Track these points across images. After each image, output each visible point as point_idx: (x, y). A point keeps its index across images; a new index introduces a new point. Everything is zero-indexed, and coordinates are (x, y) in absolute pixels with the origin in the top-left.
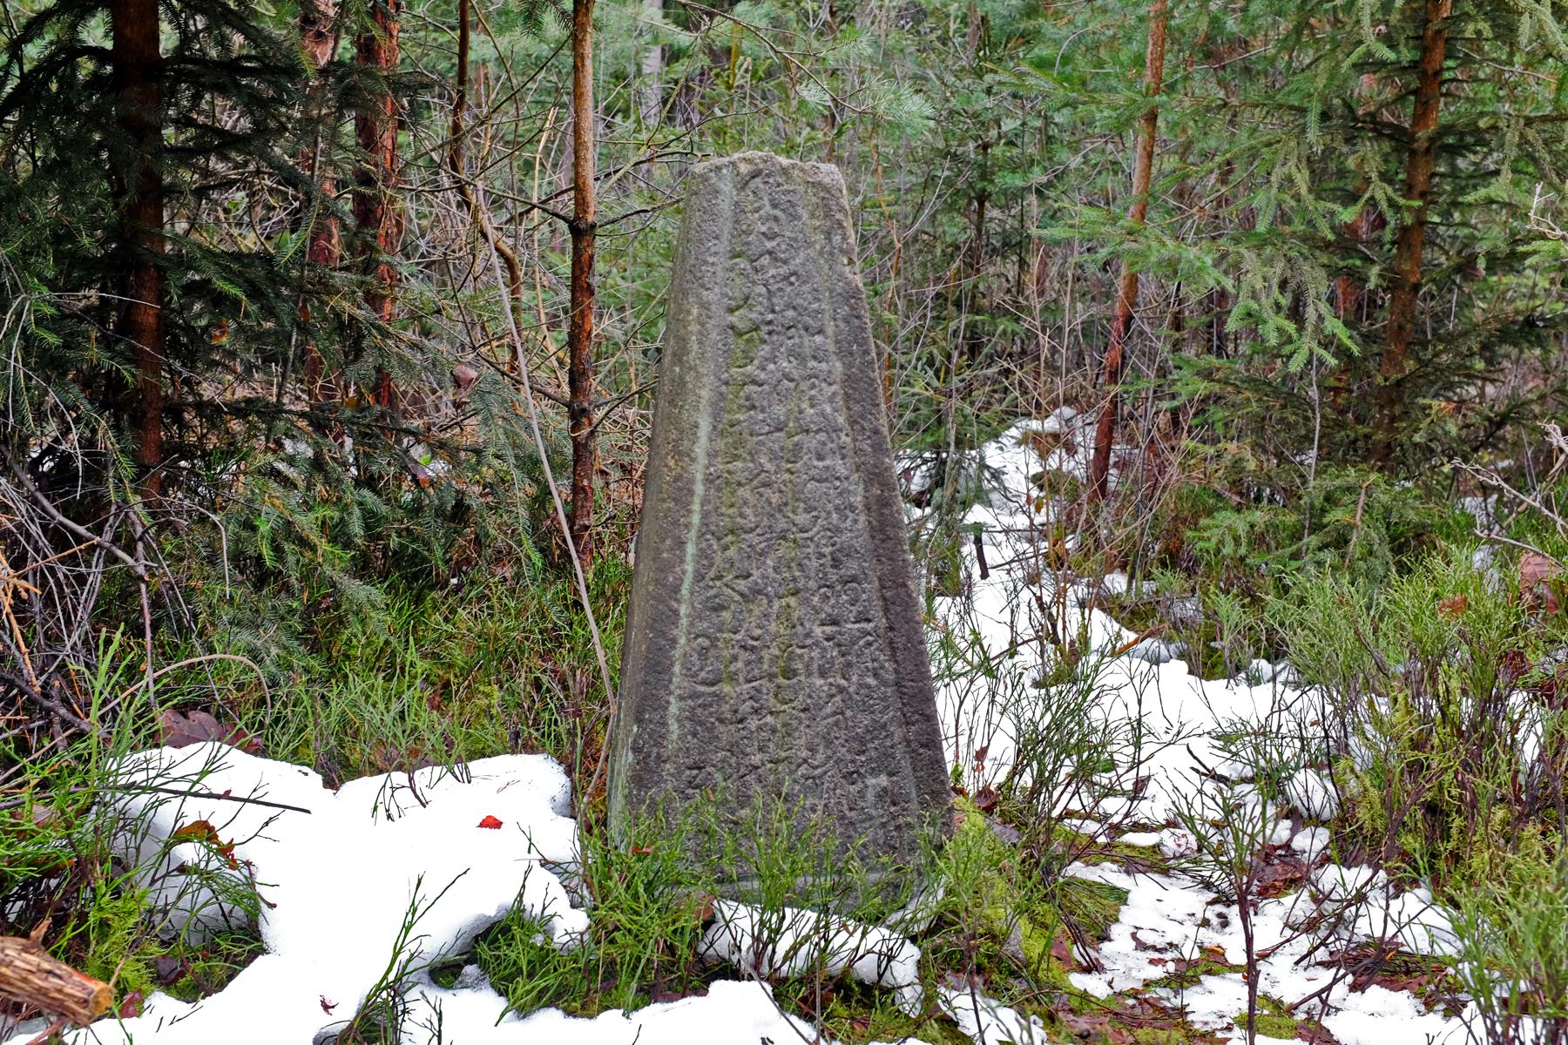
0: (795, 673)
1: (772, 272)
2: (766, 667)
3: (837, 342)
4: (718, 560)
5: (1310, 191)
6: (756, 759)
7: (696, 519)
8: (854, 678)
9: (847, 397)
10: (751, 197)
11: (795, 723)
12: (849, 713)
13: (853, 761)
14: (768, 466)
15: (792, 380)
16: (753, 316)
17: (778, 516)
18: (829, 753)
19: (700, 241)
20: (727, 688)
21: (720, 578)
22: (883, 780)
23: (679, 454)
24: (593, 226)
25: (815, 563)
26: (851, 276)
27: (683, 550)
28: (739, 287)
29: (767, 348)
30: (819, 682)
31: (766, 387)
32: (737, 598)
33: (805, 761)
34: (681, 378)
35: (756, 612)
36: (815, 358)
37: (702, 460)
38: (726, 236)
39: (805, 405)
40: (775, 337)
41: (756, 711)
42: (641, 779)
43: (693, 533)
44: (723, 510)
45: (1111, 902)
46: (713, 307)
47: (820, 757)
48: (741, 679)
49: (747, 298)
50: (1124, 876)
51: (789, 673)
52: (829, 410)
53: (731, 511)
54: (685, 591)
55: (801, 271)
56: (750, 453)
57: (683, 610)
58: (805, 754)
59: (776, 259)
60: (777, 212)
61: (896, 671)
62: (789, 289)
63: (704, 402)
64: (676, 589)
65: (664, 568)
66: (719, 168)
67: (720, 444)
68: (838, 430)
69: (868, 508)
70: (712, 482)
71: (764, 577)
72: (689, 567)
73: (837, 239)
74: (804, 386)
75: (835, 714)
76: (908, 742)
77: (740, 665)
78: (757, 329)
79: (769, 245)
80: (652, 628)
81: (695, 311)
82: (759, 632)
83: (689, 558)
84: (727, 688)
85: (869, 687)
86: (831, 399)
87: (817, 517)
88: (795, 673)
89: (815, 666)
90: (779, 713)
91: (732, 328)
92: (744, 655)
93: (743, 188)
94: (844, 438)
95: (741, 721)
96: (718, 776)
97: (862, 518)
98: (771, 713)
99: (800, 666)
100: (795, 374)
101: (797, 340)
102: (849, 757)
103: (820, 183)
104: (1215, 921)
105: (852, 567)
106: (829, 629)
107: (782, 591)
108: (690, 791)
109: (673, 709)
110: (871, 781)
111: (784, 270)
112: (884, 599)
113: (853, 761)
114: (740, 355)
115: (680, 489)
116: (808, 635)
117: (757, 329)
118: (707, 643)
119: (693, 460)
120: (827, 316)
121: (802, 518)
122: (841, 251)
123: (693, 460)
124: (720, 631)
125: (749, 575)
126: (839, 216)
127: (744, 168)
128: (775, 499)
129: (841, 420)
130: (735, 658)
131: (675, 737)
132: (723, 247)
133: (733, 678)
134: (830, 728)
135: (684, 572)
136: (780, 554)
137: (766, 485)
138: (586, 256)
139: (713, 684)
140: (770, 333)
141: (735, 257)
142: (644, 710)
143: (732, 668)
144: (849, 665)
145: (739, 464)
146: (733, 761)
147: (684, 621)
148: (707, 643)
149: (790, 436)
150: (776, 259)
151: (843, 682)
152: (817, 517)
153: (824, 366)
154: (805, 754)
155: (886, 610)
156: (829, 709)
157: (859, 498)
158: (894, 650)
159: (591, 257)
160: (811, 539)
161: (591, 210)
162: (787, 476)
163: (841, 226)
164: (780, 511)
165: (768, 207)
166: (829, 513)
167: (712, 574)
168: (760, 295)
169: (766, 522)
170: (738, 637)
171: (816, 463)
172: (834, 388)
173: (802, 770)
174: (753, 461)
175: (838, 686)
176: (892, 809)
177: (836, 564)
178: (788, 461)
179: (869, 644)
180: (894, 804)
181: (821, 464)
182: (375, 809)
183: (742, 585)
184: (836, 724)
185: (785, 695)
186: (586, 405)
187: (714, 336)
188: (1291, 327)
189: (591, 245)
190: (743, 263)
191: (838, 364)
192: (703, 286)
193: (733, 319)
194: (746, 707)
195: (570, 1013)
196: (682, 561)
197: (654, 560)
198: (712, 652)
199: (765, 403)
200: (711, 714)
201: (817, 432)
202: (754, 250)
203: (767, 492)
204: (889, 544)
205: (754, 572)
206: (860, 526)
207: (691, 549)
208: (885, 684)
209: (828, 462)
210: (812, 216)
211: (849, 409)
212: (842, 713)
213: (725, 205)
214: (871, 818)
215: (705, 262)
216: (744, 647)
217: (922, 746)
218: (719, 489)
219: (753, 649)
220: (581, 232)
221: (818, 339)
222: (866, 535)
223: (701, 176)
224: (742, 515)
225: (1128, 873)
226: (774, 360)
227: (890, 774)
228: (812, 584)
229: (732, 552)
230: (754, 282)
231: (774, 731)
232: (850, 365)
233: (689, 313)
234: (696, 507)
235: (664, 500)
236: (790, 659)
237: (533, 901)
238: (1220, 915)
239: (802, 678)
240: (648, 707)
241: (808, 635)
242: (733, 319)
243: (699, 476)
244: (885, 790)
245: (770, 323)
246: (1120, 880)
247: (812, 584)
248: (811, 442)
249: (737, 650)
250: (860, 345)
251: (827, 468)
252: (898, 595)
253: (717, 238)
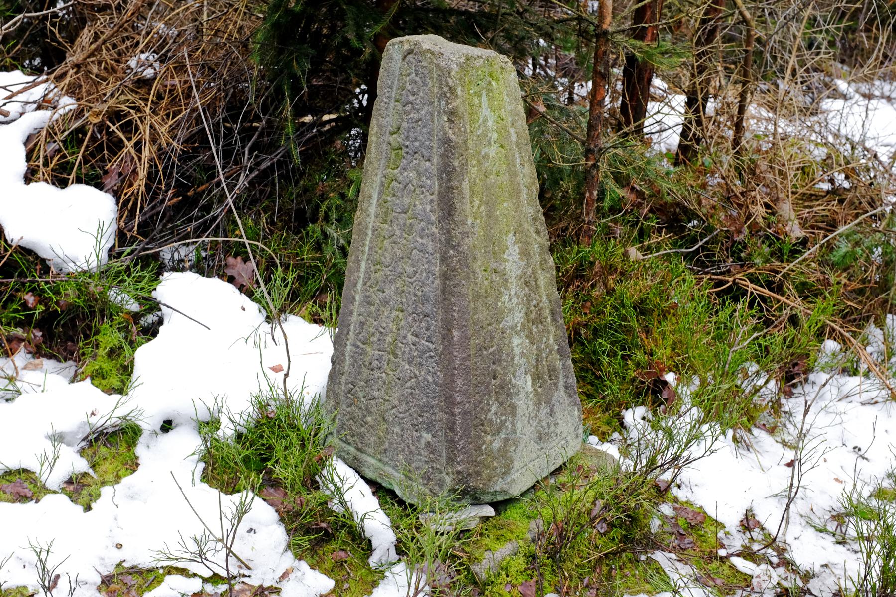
26: (447, 129)
41: (379, 368)
49: (399, 129)
57: (357, 298)
78: (401, 149)
79: (411, 98)
84: (369, 349)
102: (415, 416)
105: (428, 308)
106: (414, 339)
109: (349, 348)
110: (425, 435)
128: (399, 252)
136: (398, 285)
139: (364, 344)
151: (417, 372)
157: (437, 269)
179: (432, 357)
181: (420, 241)
184: (411, 393)
196: (359, 271)
207: (363, 265)
209: (424, 241)
221: (428, 164)
245: (407, 147)
250: (447, 175)
251: (423, 244)
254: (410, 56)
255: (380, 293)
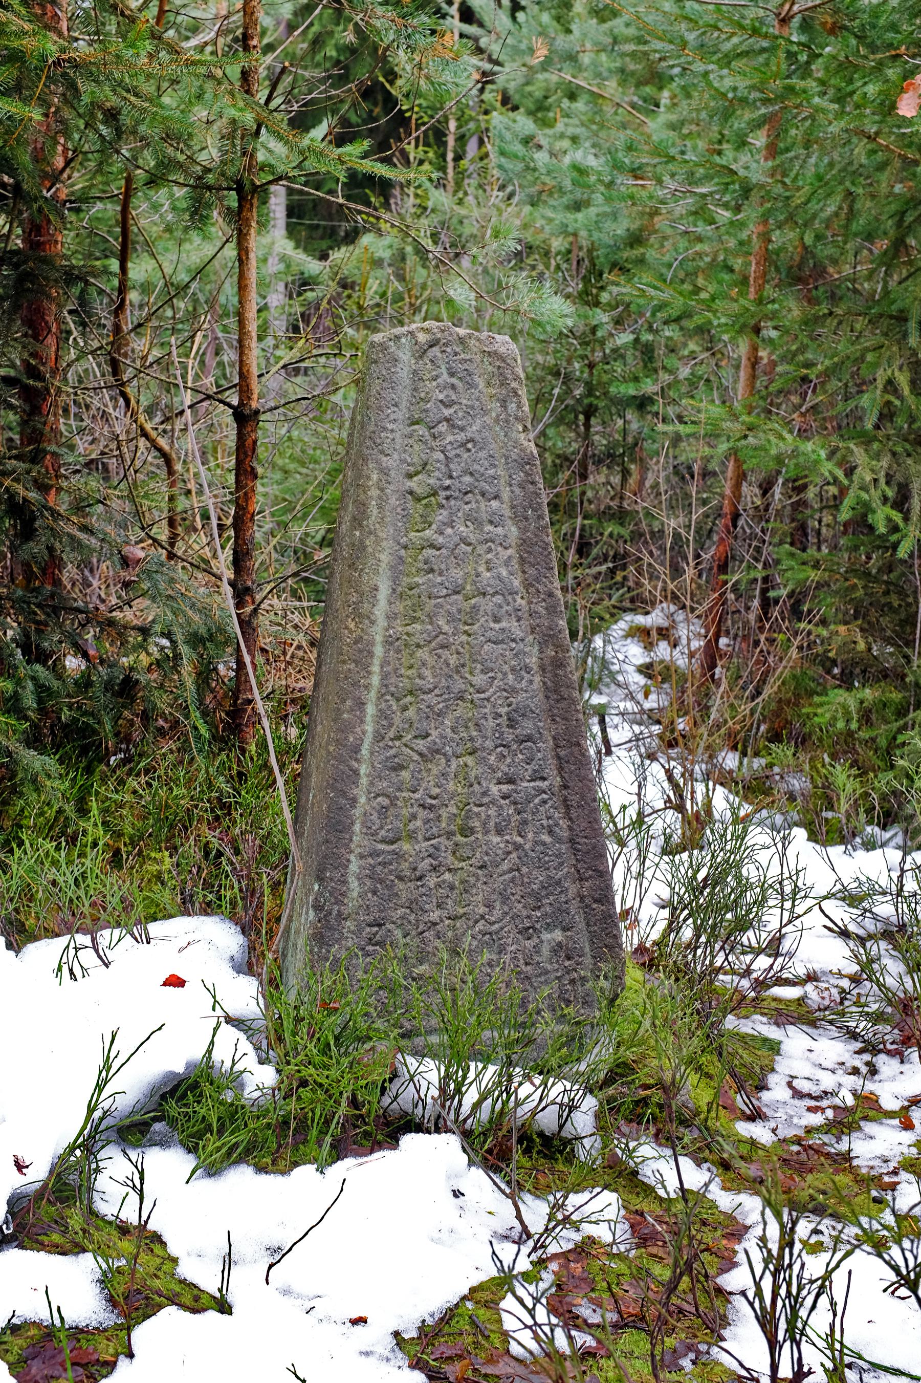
0: (472, 831)
1: (450, 438)
2: (444, 825)
3: (513, 507)
4: (397, 720)
5: (911, 392)
6: (435, 916)
7: (375, 680)
8: (530, 836)
9: (522, 560)
10: (429, 366)
11: (472, 880)
12: (525, 870)
13: (528, 917)
14: (446, 628)
15: (469, 544)
16: (431, 481)
17: (456, 677)
18: (506, 908)
19: (380, 408)
20: (406, 846)
21: (399, 738)
22: (558, 935)
23: (359, 616)
24: (257, 412)
25: (491, 723)
26: (526, 443)
27: (363, 711)
28: (417, 454)
29: (445, 513)
30: (496, 839)
31: (443, 551)
32: (416, 757)
33: (482, 917)
34: (362, 542)
35: (435, 771)
36: (491, 522)
37: (382, 622)
38: (404, 404)
39: (482, 568)
40: (453, 502)
41: (434, 869)
42: (322, 937)
43: (373, 694)
44: (403, 671)
45: (763, 1052)
46: (392, 473)
47: (497, 913)
48: (420, 838)
50: (774, 1028)
51: (466, 831)
52: (504, 573)
53: (410, 672)
54: (365, 751)
55: (477, 437)
56: (429, 616)
57: (363, 770)
58: (482, 910)
59: (453, 426)
60: (454, 380)
61: (570, 829)
62: (465, 455)
63: (383, 565)
64: (357, 749)
65: (345, 728)
66: (398, 338)
67: (400, 607)
68: (513, 593)
69: (543, 669)
70: (391, 644)
71: (442, 737)
72: (369, 728)
73: (512, 407)
74: (481, 549)
75: (511, 870)
76: (582, 898)
77: (419, 823)
78: (435, 494)
79: (447, 412)
80: (333, 788)
81: (375, 477)
82: (436, 791)
83: (368, 719)
84: (406, 846)
85: (544, 844)
86: (507, 563)
87: (494, 678)
88: (472, 831)
89: (492, 824)
90: (456, 870)
91: (411, 493)
92: (423, 814)
93: (421, 357)
94: (519, 600)
95: (420, 878)
96: (398, 933)
97: (537, 679)
98: (450, 870)
99: (477, 824)
100: (472, 538)
101: (474, 505)
102: (525, 913)
103: (495, 353)
104: (864, 1070)
105: (527, 727)
106: (505, 788)
107: (459, 750)
108: (370, 948)
109: (354, 867)
110: (546, 936)
111: (461, 437)
112: (559, 758)
113: (528, 917)
114: (419, 519)
115: (360, 651)
116: (485, 794)
117: (435, 494)
118: (385, 801)
119: (373, 622)
120: (502, 481)
121: (479, 679)
122: (517, 418)
123: (373, 622)
124: (400, 790)
125: (428, 735)
126: (514, 384)
127: (422, 338)
128: (453, 660)
129: (516, 583)
130: (414, 817)
131: (355, 894)
132: (401, 414)
133: (411, 836)
134: (506, 885)
135: (364, 733)
137: (443, 647)
138: (249, 442)
140: (447, 498)
141: (413, 424)
142: (325, 869)
143: (411, 826)
144: (525, 822)
145: (418, 626)
146: (412, 917)
147: (364, 781)
148: (385, 801)
149: (467, 599)
150: (453, 426)
151: (519, 840)
152: (494, 678)
153: (500, 530)
154: (482, 910)
155: (560, 769)
156: (505, 866)
157: (534, 660)
158: (568, 807)
159: (255, 442)
160: (488, 700)
161: (255, 396)
162: (464, 638)
163: (516, 394)
164: (458, 672)
165: (445, 376)
166: (505, 674)
167: (391, 734)
168: (438, 461)
169: (444, 683)
170: (417, 796)
171: (492, 625)
172: (510, 552)
173: (480, 926)
174: (431, 623)
175: (515, 843)
176: (567, 963)
177: (512, 723)
178: (466, 623)
179: (544, 802)
180: (569, 958)
181: (497, 626)
182: (60, 969)
183: (421, 745)
184: (513, 880)
185: (462, 852)
186: (249, 583)
187: (393, 501)
188: (897, 517)
189: (254, 430)
190: (421, 430)
191: (514, 529)
192: (382, 452)
193: (412, 484)
194: (425, 865)
195: (261, 1169)
196: (362, 722)
197: (335, 720)
198: (392, 811)
199: (443, 567)
200: (391, 872)
201: (493, 595)
202: (432, 417)
203: (445, 653)
204: (564, 704)
205: (432, 732)
206: (535, 686)
207: (370, 710)
208: (560, 841)
209: (504, 624)
210: (489, 384)
211: (524, 572)
212: (518, 870)
213: (403, 373)
214: (547, 972)
215: (384, 429)
216: (423, 806)
217: (596, 901)
218: (398, 651)
219: (431, 808)
220: (245, 418)
221: (495, 504)
222: (541, 696)
223: (381, 345)
224: (420, 676)
225: (777, 1024)
226: (451, 524)
227: (564, 929)
228: (489, 744)
229: (411, 713)
230: (432, 449)
231: (452, 888)
232: (525, 530)
233: (368, 478)
234: (376, 668)
235: (344, 662)
236: (468, 817)
237: (222, 1055)
238: (867, 1064)
239: (479, 836)
240: (327, 866)
241: (485, 794)
242: (412, 484)
243: (379, 639)
244: (559, 944)
245: (448, 488)
246: (772, 1032)
247: (489, 744)
248: (487, 605)
249: (415, 809)
250: (534, 510)
251: (503, 630)
252: (572, 754)
253: (396, 405)
254: (436, 349)
255: (420, 742)
